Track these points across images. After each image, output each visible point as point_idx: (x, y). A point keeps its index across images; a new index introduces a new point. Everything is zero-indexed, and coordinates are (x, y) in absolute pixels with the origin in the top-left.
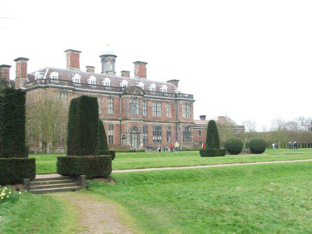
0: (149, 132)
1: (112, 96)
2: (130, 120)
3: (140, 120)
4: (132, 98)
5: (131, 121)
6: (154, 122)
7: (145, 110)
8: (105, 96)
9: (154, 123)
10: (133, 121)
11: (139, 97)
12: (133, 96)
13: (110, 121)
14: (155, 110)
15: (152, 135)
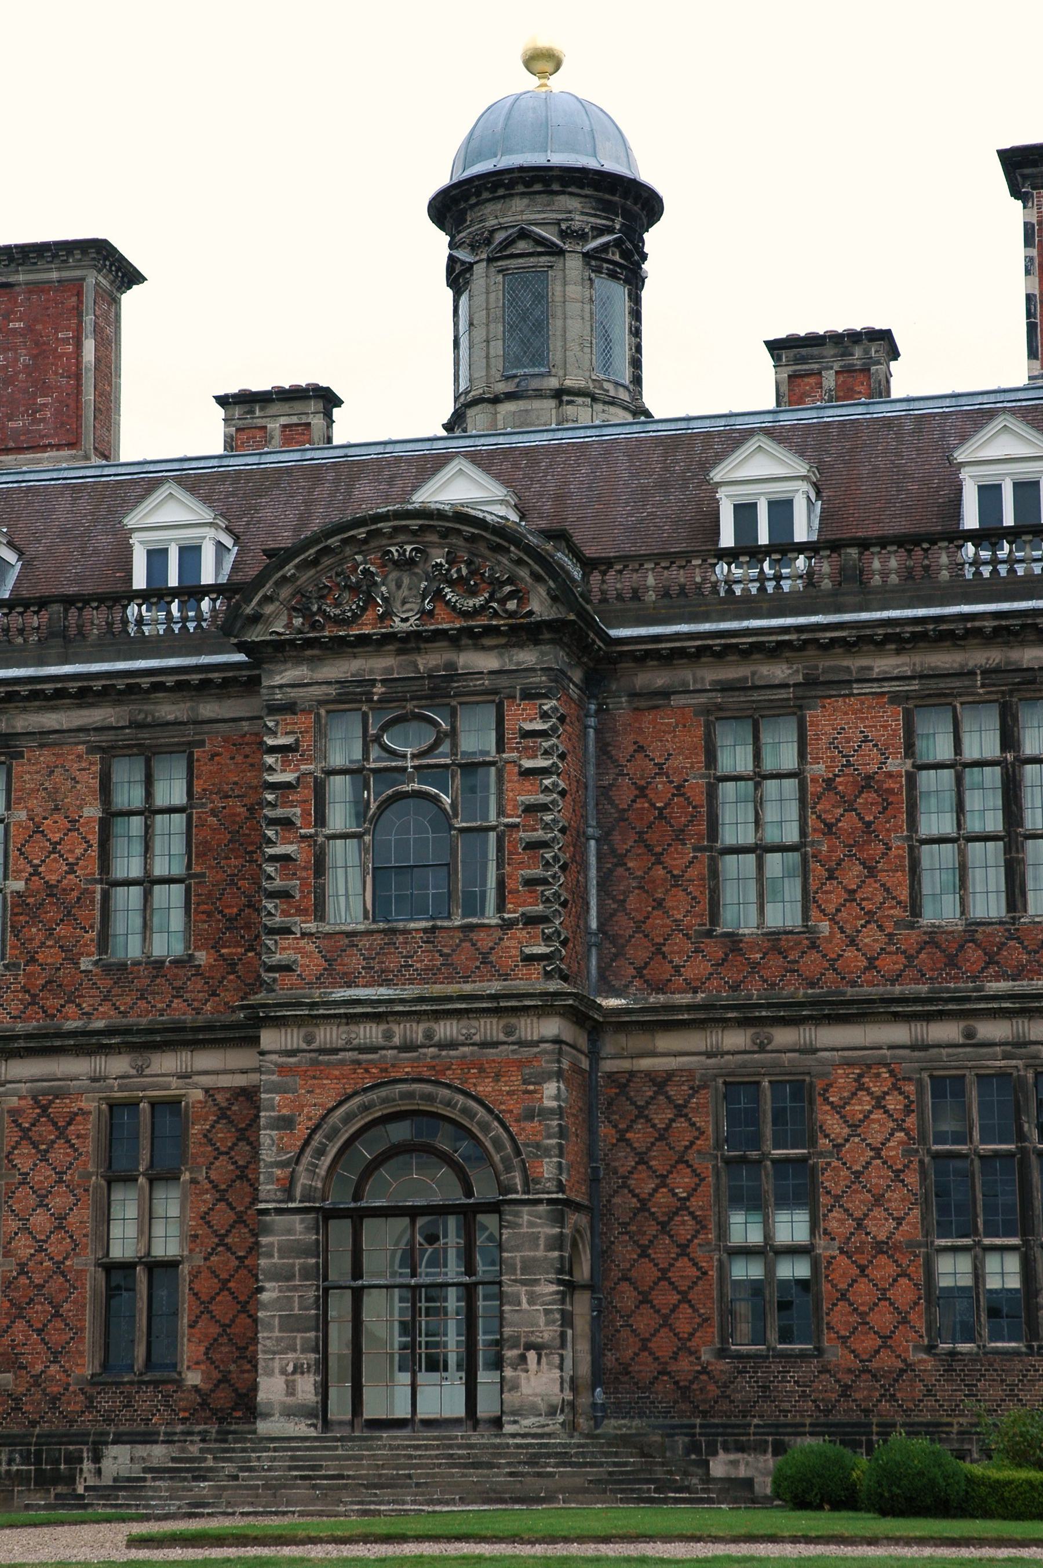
0: (827, 1180)
1: (169, 710)
2: (310, 1016)
3: (505, 1007)
4: (351, 696)
5: (328, 1035)
6: (964, 1009)
7: (760, 849)
8: (43, 737)
9: (947, 1032)
10: (370, 1033)
11: (486, 662)
12: (379, 665)
13: (119, 1065)
14: (994, 823)
15: (898, 1217)
